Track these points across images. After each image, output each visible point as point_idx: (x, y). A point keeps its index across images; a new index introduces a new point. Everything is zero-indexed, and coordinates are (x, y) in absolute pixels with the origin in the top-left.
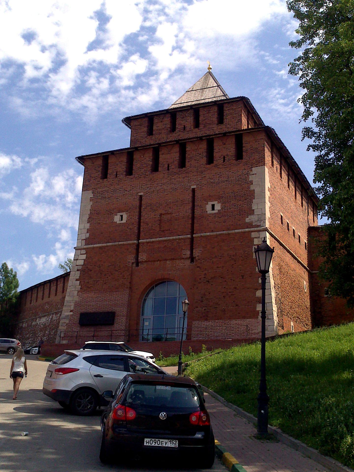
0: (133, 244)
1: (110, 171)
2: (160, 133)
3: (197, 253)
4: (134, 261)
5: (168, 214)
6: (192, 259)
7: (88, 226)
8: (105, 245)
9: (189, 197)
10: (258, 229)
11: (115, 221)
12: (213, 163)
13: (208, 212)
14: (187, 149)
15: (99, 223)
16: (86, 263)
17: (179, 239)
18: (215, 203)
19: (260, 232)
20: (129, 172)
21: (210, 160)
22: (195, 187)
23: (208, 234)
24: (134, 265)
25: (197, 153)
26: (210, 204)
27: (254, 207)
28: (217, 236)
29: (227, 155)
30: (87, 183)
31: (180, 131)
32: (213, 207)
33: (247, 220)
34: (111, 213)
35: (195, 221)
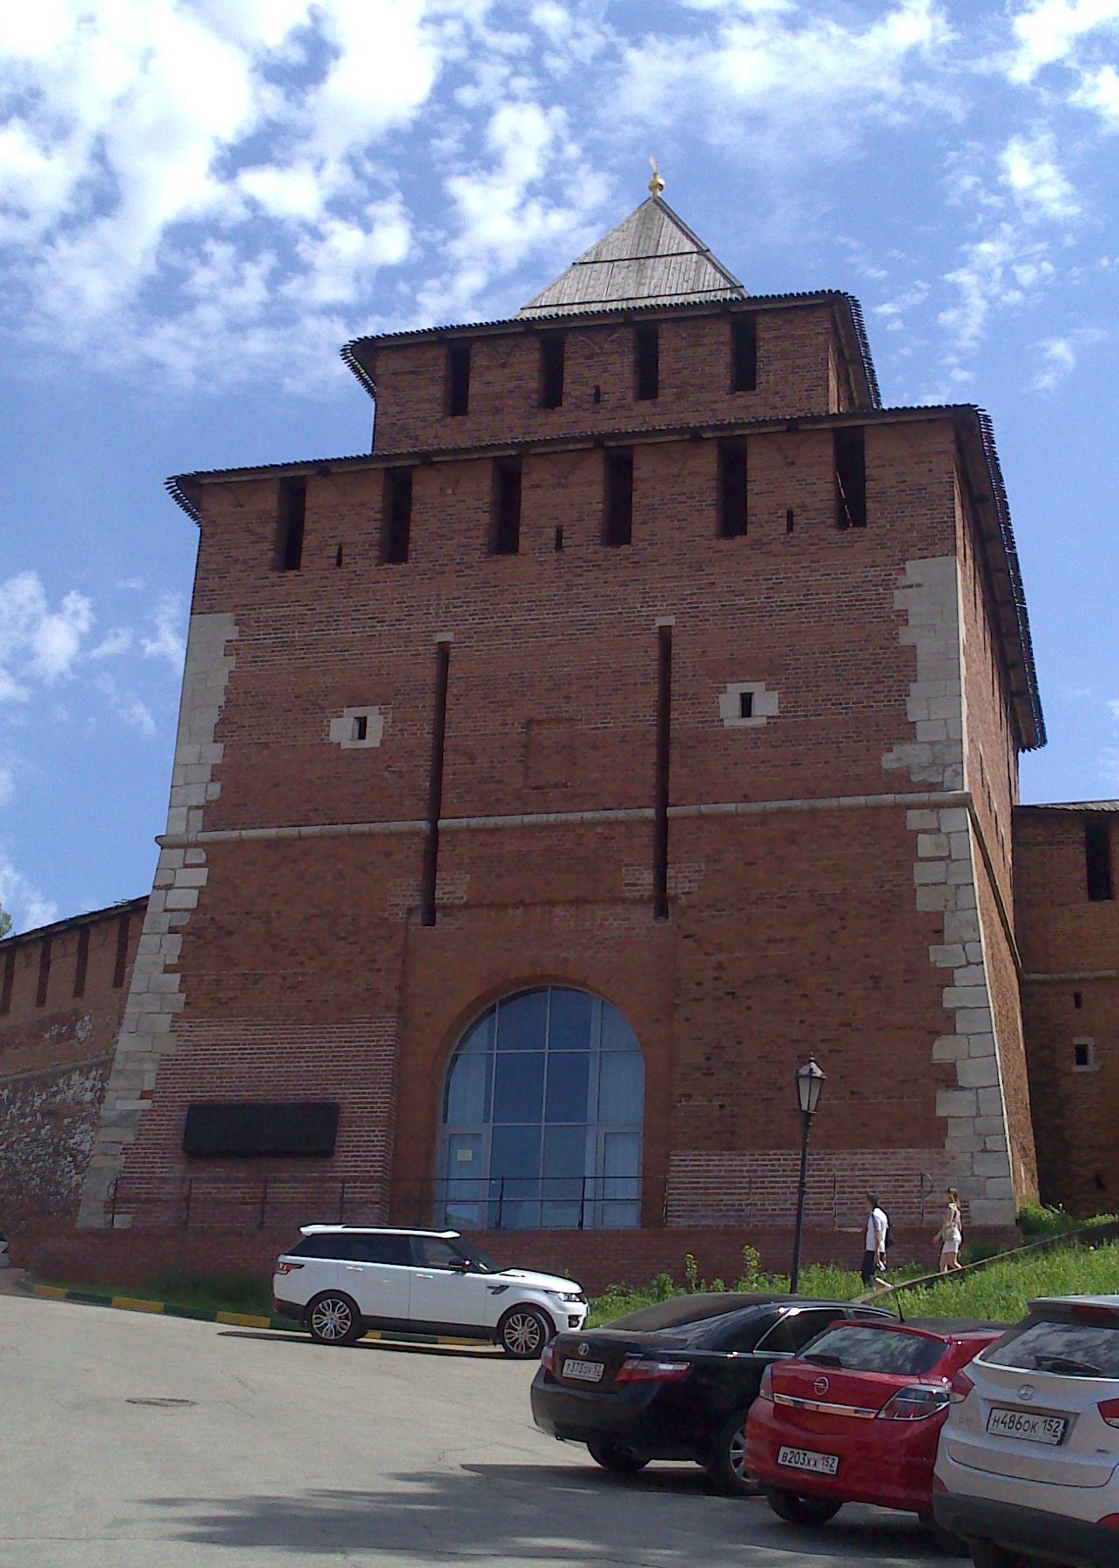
0: (413, 834)
1: (309, 541)
2: (497, 411)
3: (680, 881)
4: (416, 901)
5: (558, 720)
6: (662, 903)
7: (215, 753)
8: (294, 831)
10: (935, 796)
11: (333, 738)
12: (744, 532)
13: (726, 723)
14: (636, 474)
15: (266, 745)
16: (207, 901)
17: (609, 824)
19: (942, 812)
20: (396, 547)
21: (733, 519)
22: (670, 621)
23: (731, 807)
24: (417, 918)
25: (677, 489)
26: (735, 690)
27: (915, 712)
28: (765, 817)
29: (803, 507)
30: (214, 583)
31: (578, 407)
32: (746, 703)
33: (888, 761)
34: (316, 707)
35: (674, 756)
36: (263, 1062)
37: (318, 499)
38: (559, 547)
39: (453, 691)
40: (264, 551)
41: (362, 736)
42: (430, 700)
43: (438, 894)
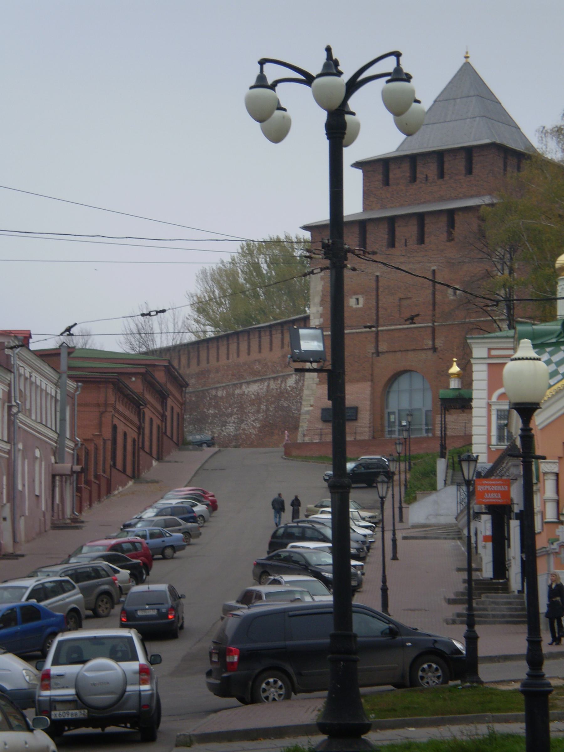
22: (435, 268)
24: (375, 355)
38: (406, 245)
39: (380, 290)
41: (358, 304)
42: (375, 293)
43: (379, 349)
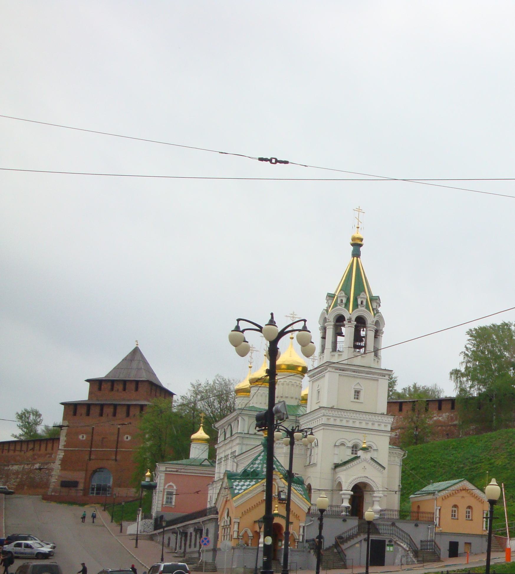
1: (78, 412)
3: (118, 457)
6: (116, 460)
9: (116, 431)
18: (128, 436)
32: (127, 438)
34: (78, 434)
36: (70, 476)
37: (78, 407)
40: (72, 413)
